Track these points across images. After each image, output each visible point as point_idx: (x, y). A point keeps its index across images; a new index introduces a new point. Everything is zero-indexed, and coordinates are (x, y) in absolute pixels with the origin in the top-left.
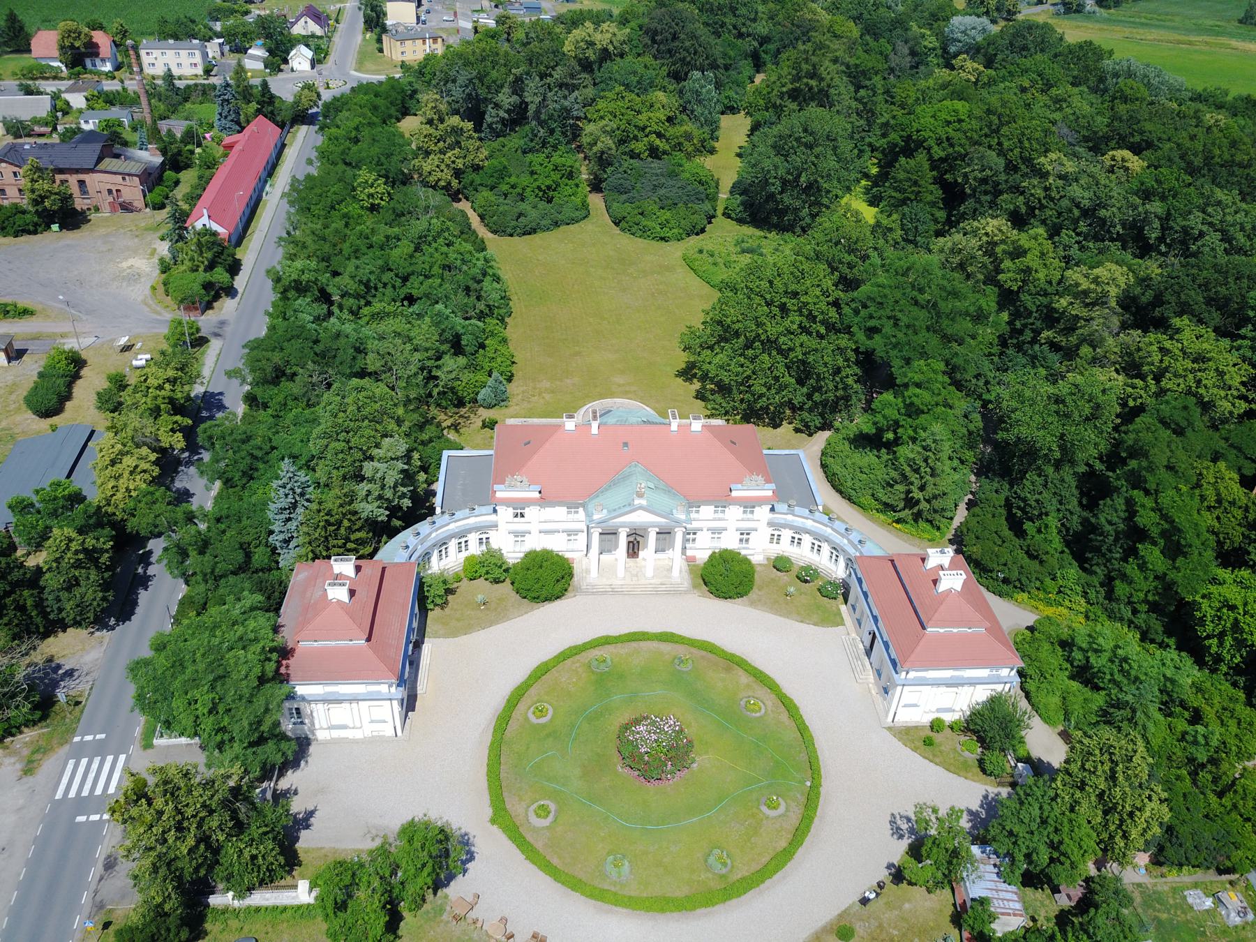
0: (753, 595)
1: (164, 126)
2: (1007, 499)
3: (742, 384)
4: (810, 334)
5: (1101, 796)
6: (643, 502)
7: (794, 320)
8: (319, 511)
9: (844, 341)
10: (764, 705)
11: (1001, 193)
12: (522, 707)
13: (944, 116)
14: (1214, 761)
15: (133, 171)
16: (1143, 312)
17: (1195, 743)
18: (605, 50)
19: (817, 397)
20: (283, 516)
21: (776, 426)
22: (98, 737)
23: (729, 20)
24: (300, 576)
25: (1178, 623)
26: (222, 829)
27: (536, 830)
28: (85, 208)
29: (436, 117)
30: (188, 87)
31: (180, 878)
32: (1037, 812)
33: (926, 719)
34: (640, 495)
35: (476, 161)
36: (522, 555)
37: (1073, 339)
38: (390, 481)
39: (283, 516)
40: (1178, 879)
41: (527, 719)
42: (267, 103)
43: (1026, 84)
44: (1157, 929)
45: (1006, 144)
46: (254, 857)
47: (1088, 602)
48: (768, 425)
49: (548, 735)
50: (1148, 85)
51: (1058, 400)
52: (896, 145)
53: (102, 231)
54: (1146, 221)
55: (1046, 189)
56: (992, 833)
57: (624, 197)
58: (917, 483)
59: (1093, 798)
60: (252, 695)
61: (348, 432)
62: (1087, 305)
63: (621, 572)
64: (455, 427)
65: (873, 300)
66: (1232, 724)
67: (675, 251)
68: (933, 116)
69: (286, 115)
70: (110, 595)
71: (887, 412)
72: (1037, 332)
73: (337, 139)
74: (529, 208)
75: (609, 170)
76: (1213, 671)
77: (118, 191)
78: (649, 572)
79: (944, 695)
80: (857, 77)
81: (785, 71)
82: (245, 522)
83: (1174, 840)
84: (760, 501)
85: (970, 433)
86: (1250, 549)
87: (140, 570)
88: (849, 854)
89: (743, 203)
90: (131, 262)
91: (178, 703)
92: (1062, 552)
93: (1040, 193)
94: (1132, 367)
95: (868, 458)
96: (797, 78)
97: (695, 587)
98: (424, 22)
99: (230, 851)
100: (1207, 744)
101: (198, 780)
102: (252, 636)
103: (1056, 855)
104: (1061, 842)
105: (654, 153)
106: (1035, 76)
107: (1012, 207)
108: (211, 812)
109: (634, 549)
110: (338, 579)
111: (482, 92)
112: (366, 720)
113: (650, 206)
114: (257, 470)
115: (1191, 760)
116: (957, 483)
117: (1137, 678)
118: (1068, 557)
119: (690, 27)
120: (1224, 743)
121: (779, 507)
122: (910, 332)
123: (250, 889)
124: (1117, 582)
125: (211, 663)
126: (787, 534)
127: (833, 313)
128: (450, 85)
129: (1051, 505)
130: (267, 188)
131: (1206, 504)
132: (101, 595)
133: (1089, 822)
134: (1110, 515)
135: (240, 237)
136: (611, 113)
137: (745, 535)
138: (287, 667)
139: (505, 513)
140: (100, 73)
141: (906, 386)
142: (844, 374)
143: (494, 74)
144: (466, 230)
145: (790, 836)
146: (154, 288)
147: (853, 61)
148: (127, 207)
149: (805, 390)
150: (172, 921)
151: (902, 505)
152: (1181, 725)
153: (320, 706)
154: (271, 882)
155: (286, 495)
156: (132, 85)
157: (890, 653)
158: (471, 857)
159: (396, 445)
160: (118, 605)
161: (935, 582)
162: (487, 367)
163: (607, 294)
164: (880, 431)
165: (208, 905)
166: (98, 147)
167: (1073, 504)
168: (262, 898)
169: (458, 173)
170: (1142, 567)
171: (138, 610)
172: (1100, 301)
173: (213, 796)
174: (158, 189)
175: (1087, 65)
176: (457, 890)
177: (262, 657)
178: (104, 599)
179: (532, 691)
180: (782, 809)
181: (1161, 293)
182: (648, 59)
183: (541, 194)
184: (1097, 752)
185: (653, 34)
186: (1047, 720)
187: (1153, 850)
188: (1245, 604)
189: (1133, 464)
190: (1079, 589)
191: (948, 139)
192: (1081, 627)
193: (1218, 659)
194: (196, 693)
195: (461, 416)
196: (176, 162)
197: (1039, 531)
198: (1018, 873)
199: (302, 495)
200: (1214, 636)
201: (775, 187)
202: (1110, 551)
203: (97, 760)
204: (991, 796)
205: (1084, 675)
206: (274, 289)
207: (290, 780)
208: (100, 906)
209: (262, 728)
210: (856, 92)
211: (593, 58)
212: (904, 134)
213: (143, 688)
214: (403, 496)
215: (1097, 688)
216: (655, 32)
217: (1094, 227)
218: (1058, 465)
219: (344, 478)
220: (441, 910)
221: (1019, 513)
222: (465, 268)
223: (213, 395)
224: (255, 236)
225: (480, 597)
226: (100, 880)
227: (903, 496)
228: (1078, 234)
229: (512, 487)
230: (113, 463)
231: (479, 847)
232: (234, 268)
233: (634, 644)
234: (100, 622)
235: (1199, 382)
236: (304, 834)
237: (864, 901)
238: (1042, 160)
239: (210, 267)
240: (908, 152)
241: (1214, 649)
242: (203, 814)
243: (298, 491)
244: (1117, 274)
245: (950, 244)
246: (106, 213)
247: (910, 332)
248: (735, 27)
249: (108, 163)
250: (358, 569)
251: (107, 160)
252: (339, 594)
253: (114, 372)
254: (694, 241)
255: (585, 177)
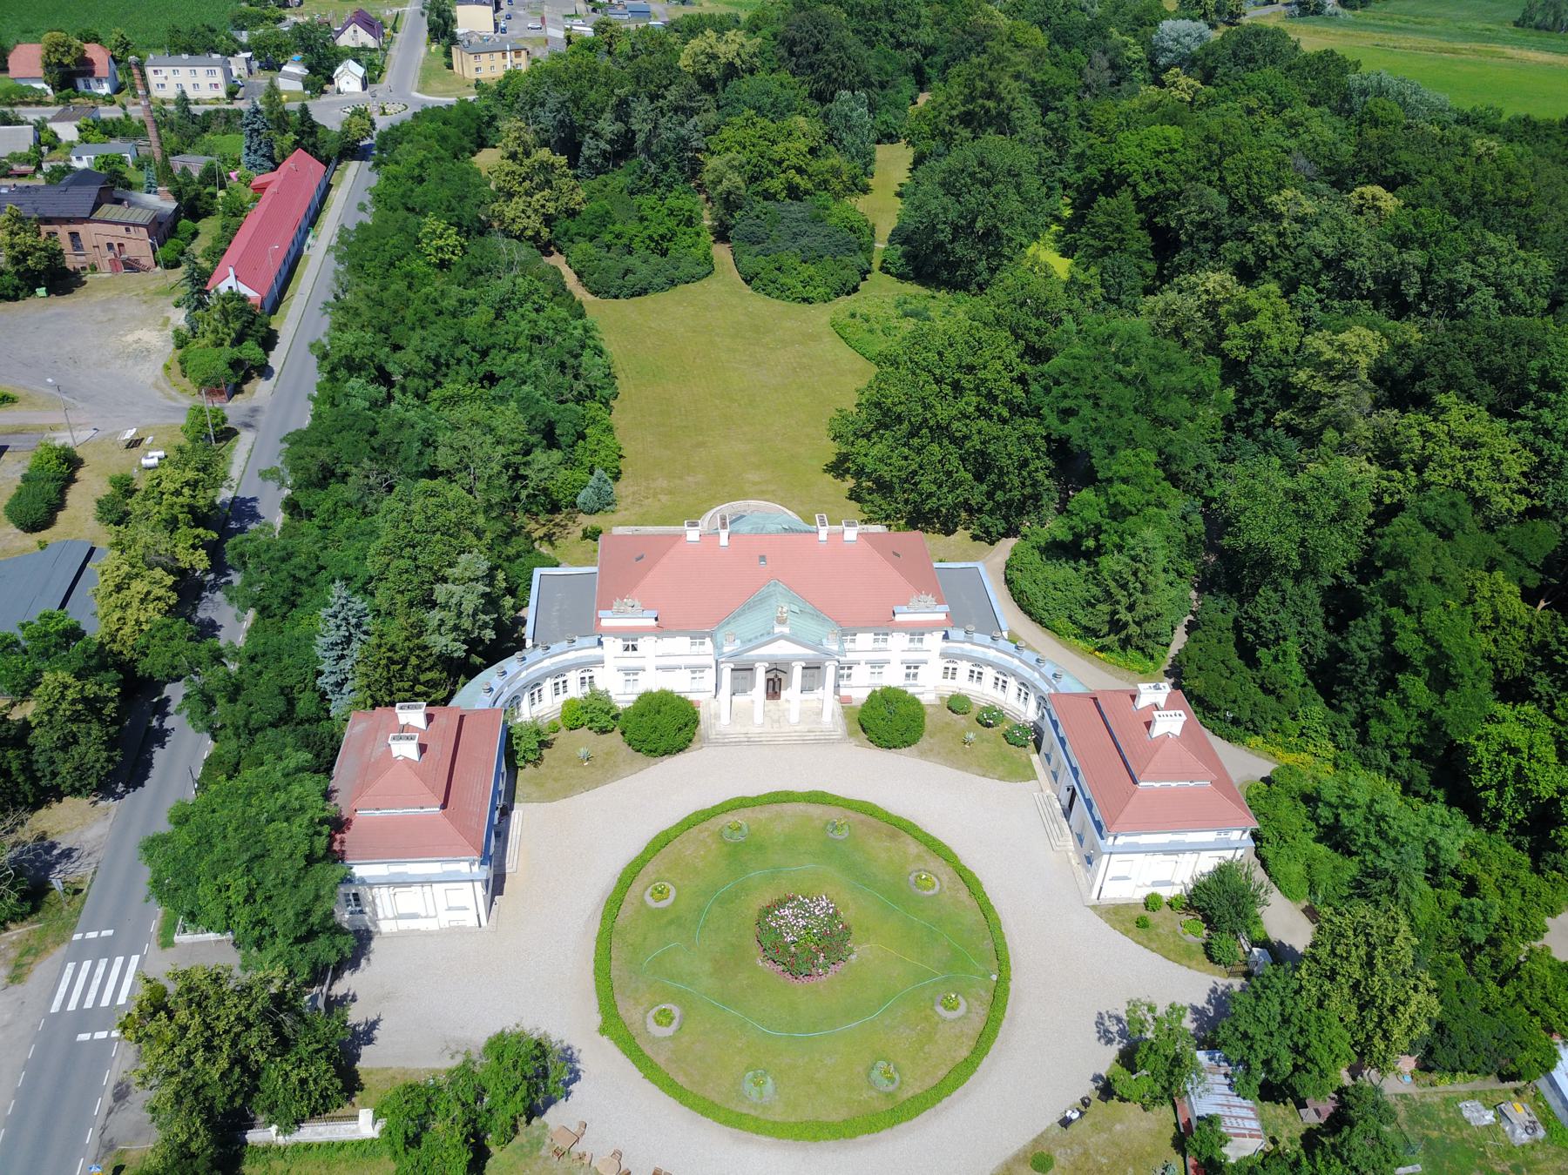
0: (924, 742)
1: (177, 163)
2: (1236, 620)
3: (906, 481)
4: (990, 417)
5: (1355, 987)
6: (786, 630)
7: (970, 401)
8: (379, 646)
9: (1032, 426)
10: (939, 880)
11: (1224, 239)
12: (636, 888)
13: (1153, 144)
14: (1493, 942)
15: (139, 221)
16: (1400, 388)
17: (1471, 919)
18: (731, 64)
19: (999, 496)
20: (334, 653)
21: (948, 533)
22: (104, 933)
23: (885, 26)
24: (357, 729)
25: (1448, 772)
26: (260, 1046)
27: (656, 1041)
28: (79, 266)
29: (520, 150)
30: (207, 114)
31: (210, 1110)
32: (1278, 1008)
33: (1139, 895)
34: (782, 622)
35: (572, 204)
36: (634, 698)
37: (1315, 422)
38: (468, 608)
39: (334, 653)
40: (1451, 1088)
41: (643, 903)
42: (307, 133)
43: (1254, 104)
44: (1427, 1151)
45: (1230, 179)
46: (303, 1082)
47: (1337, 747)
48: (939, 531)
49: (670, 922)
50: (1403, 104)
51: (1297, 497)
52: (1094, 181)
53: (101, 296)
54: (1403, 273)
55: (1280, 235)
56: (1222, 1035)
57: (757, 248)
58: (1125, 601)
59: (1346, 991)
60: (298, 878)
61: (414, 547)
62: (1331, 379)
63: (758, 717)
64: (549, 538)
65: (1067, 374)
66: (1515, 894)
67: (821, 315)
68: (1139, 145)
69: (332, 148)
70: (117, 755)
71: (1087, 514)
72: (1270, 413)
73: (396, 178)
74: (638, 263)
75: (737, 215)
76: (1492, 829)
77: (120, 245)
78: (794, 717)
79: (1160, 864)
80: (1045, 97)
81: (955, 90)
82: (286, 661)
83: (1446, 1040)
84: (931, 627)
85: (1189, 538)
86: (1535, 678)
87: (155, 723)
88: (1045, 1064)
89: (904, 255)
90: (138, 334)
91: (205, 891)
92: (1305, 685)
93: (1271, 239)
94: (1388, 456)
95: (1063, 571)
96: (971, 99)
97: (851, 734)
98: (504, 31)
99: (273, 1076)
100: (1486, 920)
101: (231, 986)
102: (296, 805)
103: (1301, 1061)
104: (1307, 1046)
105: (794, 192)
106: (1264, 94)
107: (1238, 257)
108: (249, 1026)
109: (774, 688)
110: (404, 731)
111: (578, 118)
112: (442, 906)
113: (790, 260)
114: (300, 595)
115: (1466, 941)
116: (1175, 600)
117: (1396, 840)
118: (1311, 691)
119: (836, 35)
120: (1505, 919)
121: (953, 633)
122: (1114, 414)
123: (299, 1122)
124: (1373, 722)
125: (245, 840)
126: (964, 667)
127: (1018, 392)
128: (537, 109)
129: (1291, 628)
130: (309, 240)
131: (1480, 623)
132: (105, 754)
133: (1342, 1020)
134: (1363, 638)
135: (276, 303)
136: (739, 143)
137: (912, 668)
138: (342, 842)
139: (613, 646)
140: (95, 97)
141: (1110, 481)
142: (1032, 467)
143: (592, 95)
144: (560, 291)
145: (973, 1043)
146: (167, 368)
147: (1038, 77)
148: (131, 266)
149: (984, 488)
150: (201, 1164)
151: (1106, 629)
152: (1453, 898)
153: (384, 890)
154: (326, 1111)
155: (338, 627)
156: (137, 112)
157: (1093, 813)
158: (576, 1076)
159: (475, 562)
160: (127, 767)
161: (1148, 725)
162: (587, 461)
163: (738, 370)
164: (1078, 537)
165: (246, 1143)
166: (94, 190)
167: (1318, 626)
168: (314, 1132)
169: (548, 220)
170: (1403, 703)
171: (152, 773)
172: (1348, 374)
173: (250, 1005)
174: (171, 243)
175: (1327, 80)
176: (555, 1117)
177: (311, 831)
178: (109, 760)
179: (650, 867)
180: (962, 1010)
181: (1422, 364)
182: (784, 76)
183: (653, 245)
184: (1350, 933)
185: (790, 44)
186: (1288, 894)
187: (1420, 1053)
188: (1530, 747)
189: (1390, 575)
190: (1326, 730)
191: (1158, 173)
192: (1328, 781)
193: (1497, 815)
194: (227, 878)
195: (557, 525)
196: (193, 208)
197: (1276, 660)
198: (1255, 1084)
199: (358, 626)
200: (1492, 787)
201: (945, 235)
202: (1364, 684)
203: (103, 963)
204: (1220, 988)
205: (1335, 837)
206: (319, 367)
207: (347, 983)
208: (110, 1146)
209: (311, 920)
210: (1044, 114)
211: (715, 74)
212: (1104, 167)
213: (160, 871)
214: (485, 625)
215: (1350, 854)
216: (793, 43)
217: (1339, 281)
218: (1298, 578)
219: (411, 605)
220: (539, 1143)
221: (1251, 638)
222: (559, 339)
223: (244, 501)
224: (295, 300)
225: (582, 751)
226: (109, 1114)
227: (1107, 618)
228: (1319, 291)
229: (621, 613)
230: (119, 588)
231: (586, 1064)
232: (269, 341)
233: (776, 807)
234: (105, 789)
235: (1469, 473)
236: (365, 1050)
237: (1066, 1122)
238: (1275, 198)
239: (239, 340)
240: (1109, 189)
241: (1492, 803)
242: (237, 1029)
243: (353, 621)
244: (1368, 341)
245: (1161, 305)
246: (105, 273)
247: (1114, 414)
248: (892, 35)
249: (107, 210)
250: (430, 718)
251: (106, 207)
252: (406, 750)
253: (118, 474)
254: (844, 302)
255: (707, 223)
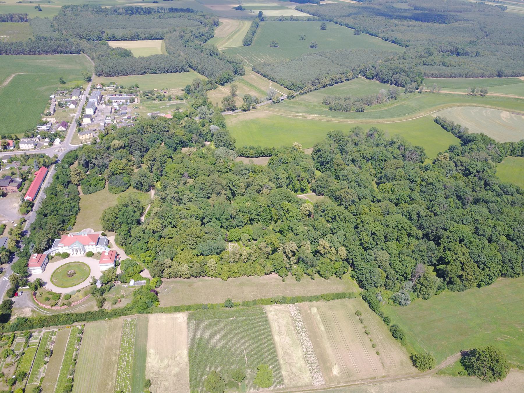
53: (10, 197)
148: (15, 192)
160: (10, 260)
207: (29, 278)
234: (8, 263)
252: (34, 258)
